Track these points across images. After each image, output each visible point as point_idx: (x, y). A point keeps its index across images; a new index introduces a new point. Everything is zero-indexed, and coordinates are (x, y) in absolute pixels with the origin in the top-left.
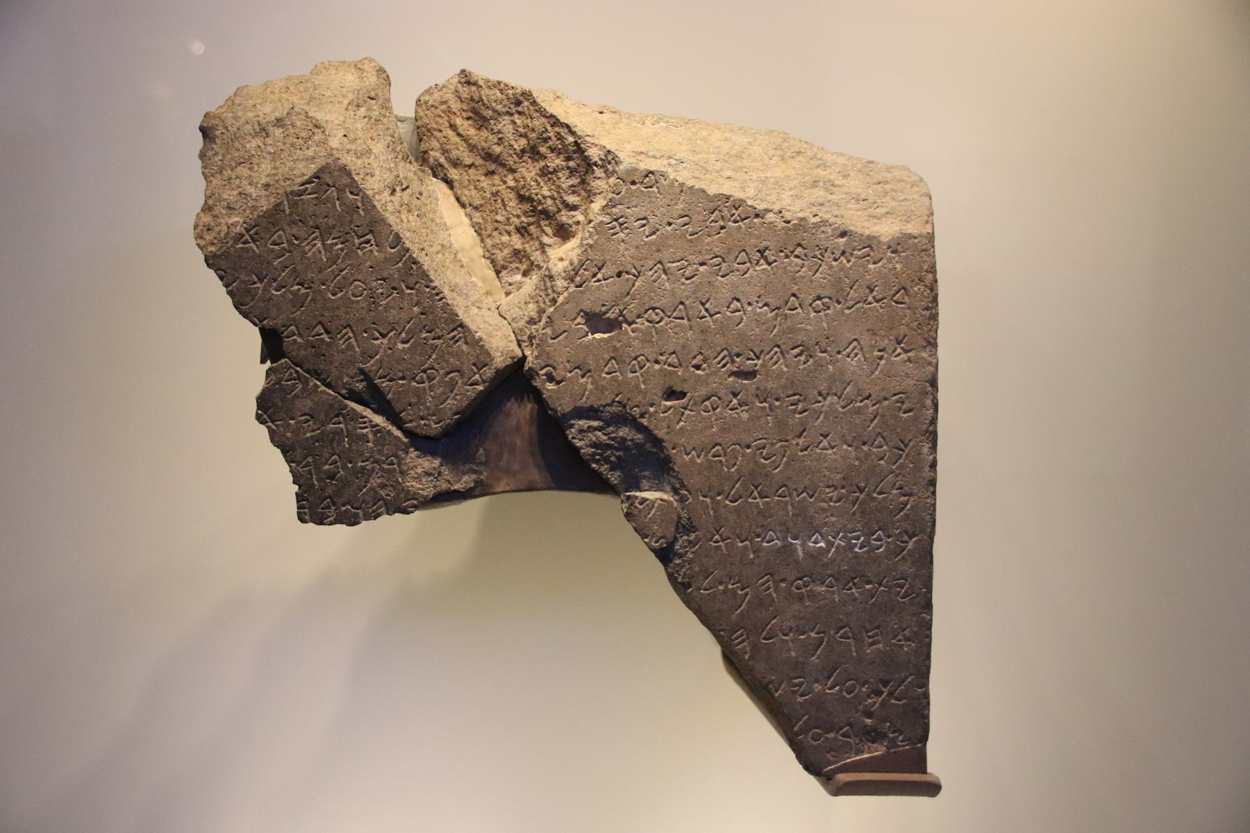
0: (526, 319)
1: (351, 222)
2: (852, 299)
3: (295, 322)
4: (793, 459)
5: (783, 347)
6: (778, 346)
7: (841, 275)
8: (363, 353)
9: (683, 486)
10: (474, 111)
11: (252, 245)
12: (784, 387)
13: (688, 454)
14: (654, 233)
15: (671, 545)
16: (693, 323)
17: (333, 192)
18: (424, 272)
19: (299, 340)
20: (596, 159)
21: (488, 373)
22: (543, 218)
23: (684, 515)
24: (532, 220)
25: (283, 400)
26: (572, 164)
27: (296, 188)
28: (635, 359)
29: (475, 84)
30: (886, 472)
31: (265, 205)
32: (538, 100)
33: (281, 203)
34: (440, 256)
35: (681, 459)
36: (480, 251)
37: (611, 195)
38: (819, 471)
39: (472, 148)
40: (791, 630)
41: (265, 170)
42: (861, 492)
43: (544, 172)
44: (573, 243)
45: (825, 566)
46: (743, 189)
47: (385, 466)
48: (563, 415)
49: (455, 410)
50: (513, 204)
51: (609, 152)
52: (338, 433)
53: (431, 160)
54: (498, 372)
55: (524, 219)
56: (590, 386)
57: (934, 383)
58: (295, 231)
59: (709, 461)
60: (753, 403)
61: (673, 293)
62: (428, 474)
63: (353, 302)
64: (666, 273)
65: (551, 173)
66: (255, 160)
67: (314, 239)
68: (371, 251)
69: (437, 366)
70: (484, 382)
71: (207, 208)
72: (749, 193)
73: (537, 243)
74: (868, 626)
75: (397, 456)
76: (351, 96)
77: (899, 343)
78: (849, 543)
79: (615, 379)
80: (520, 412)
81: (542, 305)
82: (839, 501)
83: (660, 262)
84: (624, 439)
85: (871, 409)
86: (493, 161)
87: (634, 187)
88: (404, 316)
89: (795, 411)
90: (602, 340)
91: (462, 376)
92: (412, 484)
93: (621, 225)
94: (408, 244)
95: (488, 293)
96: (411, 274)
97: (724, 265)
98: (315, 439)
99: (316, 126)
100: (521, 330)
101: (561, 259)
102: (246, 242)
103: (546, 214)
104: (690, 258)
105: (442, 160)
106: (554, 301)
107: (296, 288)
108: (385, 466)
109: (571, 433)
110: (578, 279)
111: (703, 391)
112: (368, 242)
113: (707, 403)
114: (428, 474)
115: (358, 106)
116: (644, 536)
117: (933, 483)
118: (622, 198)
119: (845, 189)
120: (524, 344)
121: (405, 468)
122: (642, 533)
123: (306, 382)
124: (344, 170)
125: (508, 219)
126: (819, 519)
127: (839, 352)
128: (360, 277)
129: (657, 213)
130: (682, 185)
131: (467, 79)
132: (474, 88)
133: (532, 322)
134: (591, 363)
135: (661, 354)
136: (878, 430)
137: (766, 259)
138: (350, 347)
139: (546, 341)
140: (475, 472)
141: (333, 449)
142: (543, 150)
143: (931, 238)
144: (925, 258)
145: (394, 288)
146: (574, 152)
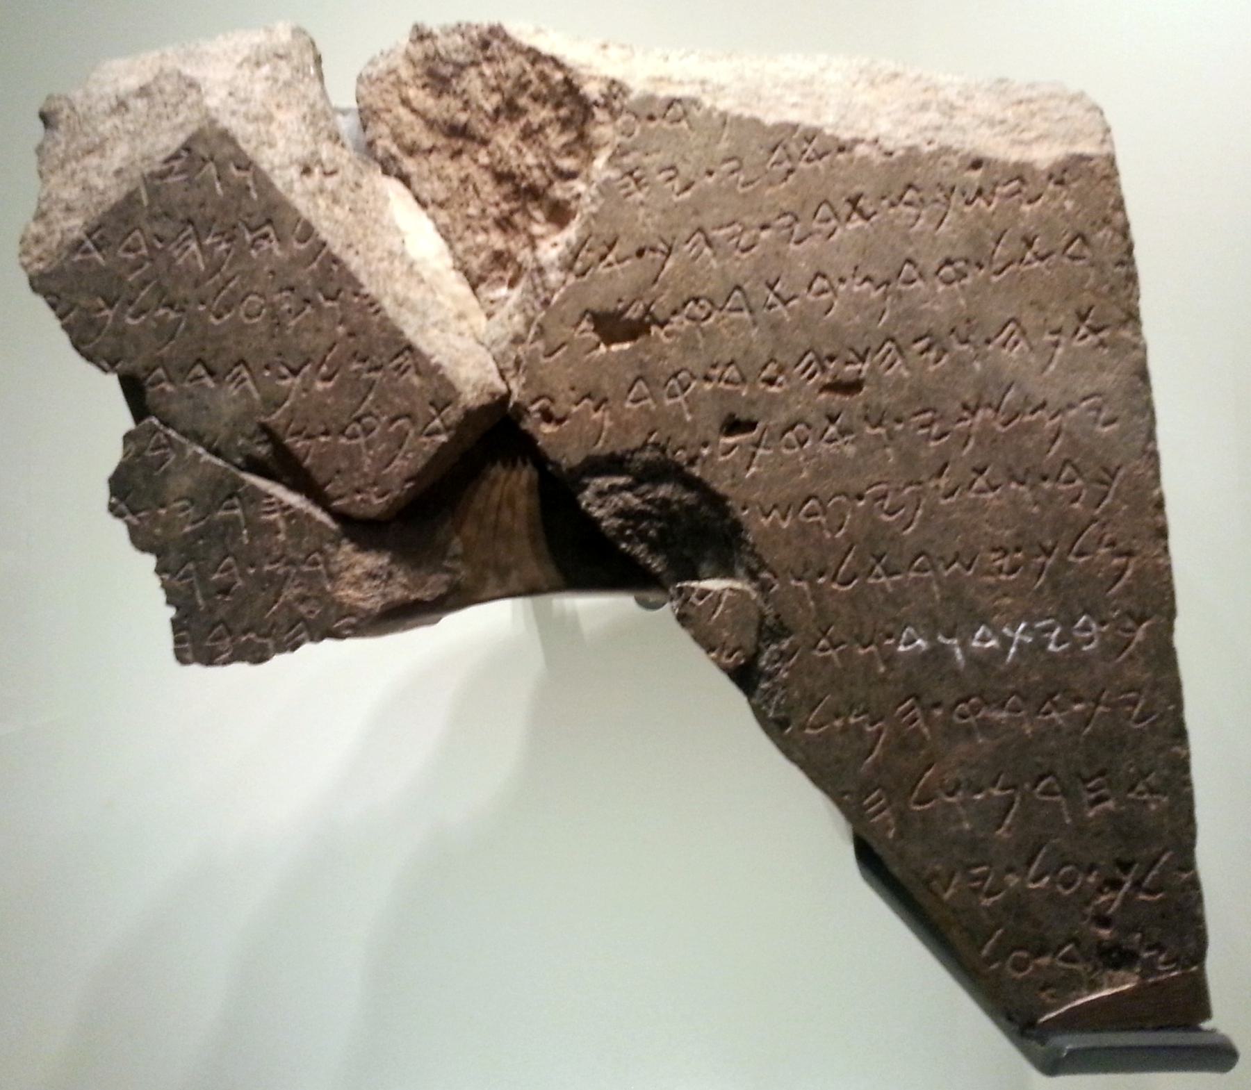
0: (510, 337)
1: (239, 209)
2: (1000, 259)
3: (161, 362)
4: (932, 511)
5: (900, 341)
6: (893, 340)
7: (980, 224)
8: (265, 400)
9: (763, 566)
10: (431, 73)
11: (97, 256)
12: (908, 401)
14: (687, 188)
15: (753, 659)
17: (211, 169)
21: (453, 415)
22: (528, 196)
23: (769, 611)
24: (514, 205)
25: (148, 478)
26: (563, 112)
27: (157, 168)
29: (430, 36)
30: (1086, 520)
31: (114, 196)
33: (137, 190)
34: (385, 264)
35: (757, 525)
36: (449, 261)
38: (975, 526)
39: (431, 124)
41: (119, 154)
42: (1048, 553)
43: (529, 134)
46: (818, 116)
47: (306, 569)
48: (571, 470)
49: (406, 475)
51: (613, 82)
53: (380, 153)
54: (469, 414)
55: (505, 207)
56: (608, 424)
57: (1143, 374)
58: (157, 228)
59: (800, 524)
60: (861, 430)
61: (723, 273)
62: (371, 576)
63: (246, 326)
66: (108, 145)
67: (185, 239)
68: (270, 251)
69: (376, 411)
70: (447, 429)
71: (41, 216)
72: (829, 121)
73: (524, 237)
75: (322, 552)
76: (246, 52)
77: (1083, 318)
79: (645, 410)
80: (511, 485)
81: (531, 313)
82: (1013, 570)
84: (666, 502)
85: (1049, 424)
86: (459, 134)
87: (652, 125)
88: (323, 341)
89: (928, 437)
90: (621, 352)
91: (414, 423)
92: (348, 594)
93: (637, 181)
94: (324, 236)
96: (331, 278)
98: (198, 535)
100: (504, 354)
101: (555, 245)
102: (87, 251)
103: (535, 193)
104: (747, 220)
105: (394, 150)
106: (546, 303)
107: (161, 312)
108: (306, 569)
110: (579, 266)
111: (782, 417)
112: (266, 236)
113: (789, 435)
115: (258, 64)
116: (710, 649)
117: (1162, 533)
120: (508, 375)
121: (335, 568)
122: (707, 642)
123: (181, 449)
124: (226, 137)
125: (484, 211)
126: (985, 602)
127: (988, 342)
128: (256, 288)
129: (690, 158)
130: (724, 115)
131: (421, 36)
132: (428, 43)
133: (517, 340)
134: (607, 386)
136: (1065, 456)
138: (246, 392)
139: (537, 360)
140: (447, 570)
141: (225, 548)
142: (523, 101)
144: (1109, 189)
145: (307, 301)
146: (565, 94)
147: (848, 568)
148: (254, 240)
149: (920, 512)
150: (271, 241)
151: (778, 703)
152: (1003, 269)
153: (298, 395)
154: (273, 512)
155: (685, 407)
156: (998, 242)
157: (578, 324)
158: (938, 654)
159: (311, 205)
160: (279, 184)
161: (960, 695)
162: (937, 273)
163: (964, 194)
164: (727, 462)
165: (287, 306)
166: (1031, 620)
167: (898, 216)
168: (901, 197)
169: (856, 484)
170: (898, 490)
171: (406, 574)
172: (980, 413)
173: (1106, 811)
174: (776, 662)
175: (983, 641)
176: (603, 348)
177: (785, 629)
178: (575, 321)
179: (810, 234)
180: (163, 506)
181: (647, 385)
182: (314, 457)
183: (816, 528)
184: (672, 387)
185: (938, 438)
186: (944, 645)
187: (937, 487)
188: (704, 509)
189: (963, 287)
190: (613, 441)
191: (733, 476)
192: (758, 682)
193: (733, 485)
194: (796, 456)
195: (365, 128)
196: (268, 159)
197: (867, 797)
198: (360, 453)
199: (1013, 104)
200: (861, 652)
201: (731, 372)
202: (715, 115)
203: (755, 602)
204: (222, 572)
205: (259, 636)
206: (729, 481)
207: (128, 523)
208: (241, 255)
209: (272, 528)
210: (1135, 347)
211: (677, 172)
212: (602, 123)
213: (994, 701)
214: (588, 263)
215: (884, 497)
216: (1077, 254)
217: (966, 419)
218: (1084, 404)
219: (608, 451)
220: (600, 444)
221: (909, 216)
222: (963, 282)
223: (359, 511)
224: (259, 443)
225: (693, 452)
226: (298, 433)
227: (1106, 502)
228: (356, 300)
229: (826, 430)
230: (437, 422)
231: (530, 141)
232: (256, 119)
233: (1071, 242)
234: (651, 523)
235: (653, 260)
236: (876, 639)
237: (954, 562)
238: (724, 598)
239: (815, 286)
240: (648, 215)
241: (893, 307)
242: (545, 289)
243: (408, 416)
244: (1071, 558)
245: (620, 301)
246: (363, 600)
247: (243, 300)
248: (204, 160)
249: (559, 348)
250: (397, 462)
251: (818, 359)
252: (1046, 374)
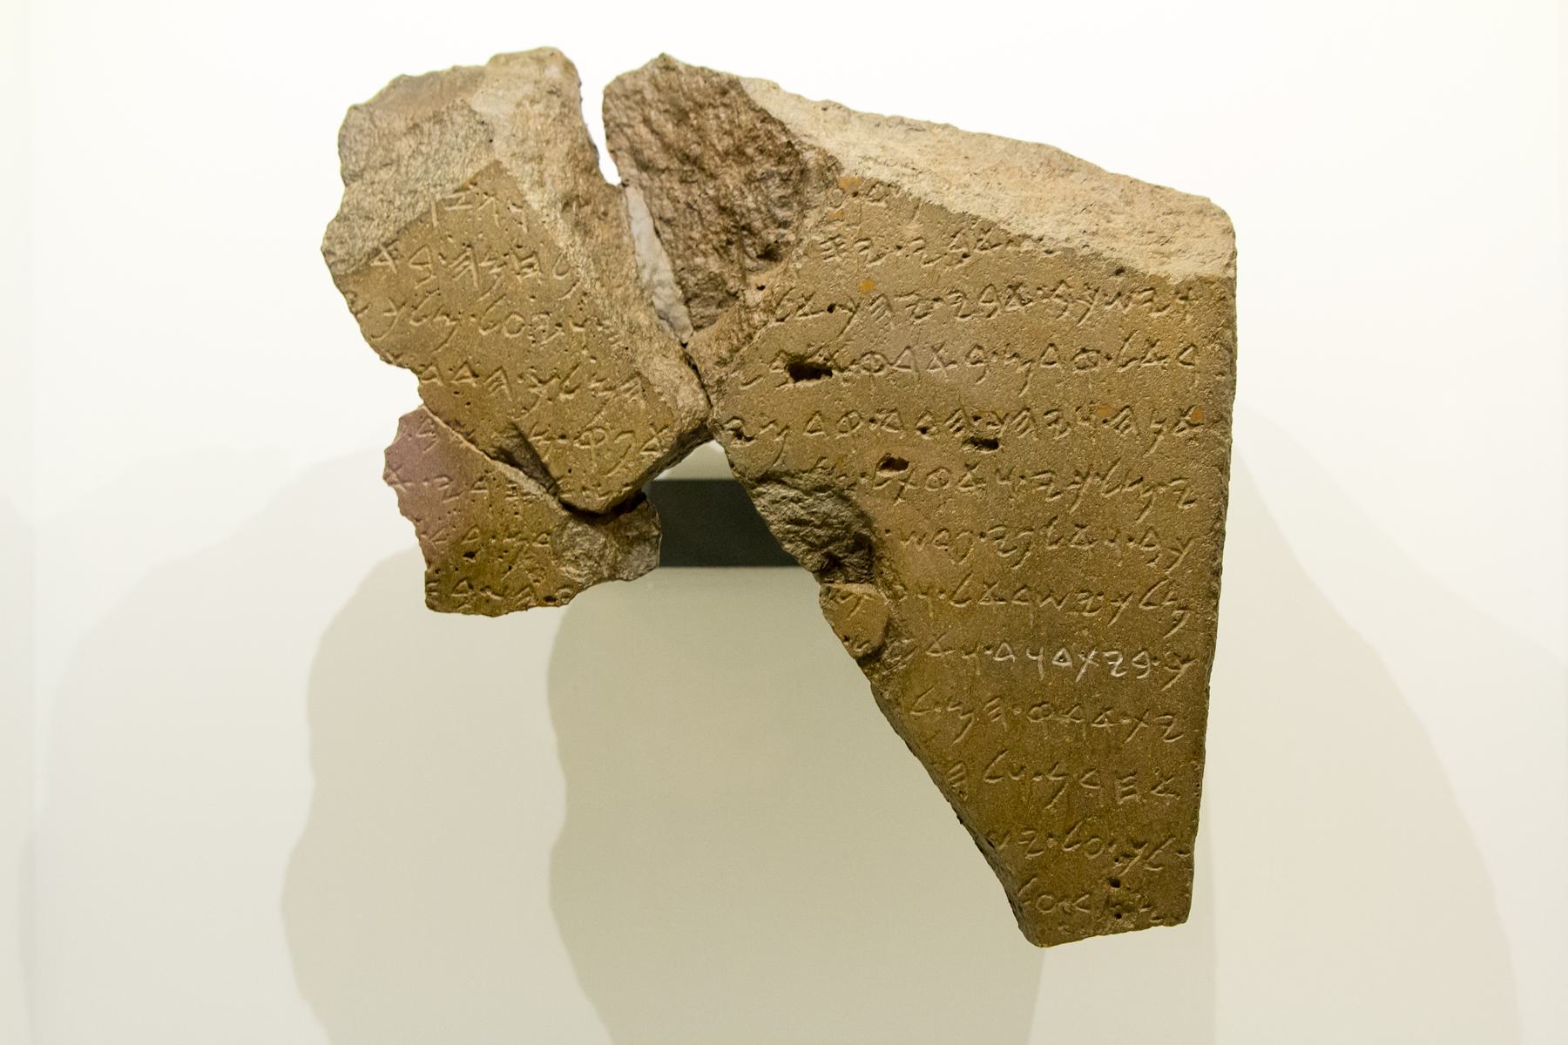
14: (879, 257)
26: (784, 169)
32: (749, 91)
39: (667, 147)
43: (749, 179)
50: (712, 216)
78: (1103, 664)
86: (692, 164)
90: (807, 389)
109: (760, 504)
117: (1215, 595)
118: (843, 212)
131: (666, 64)
132: (673, 74)
135: (879, 411)
142: (750, 151)
143: (1230, 283)
149: (1028, 554)
167: (1049, 305)
172: (1089, 480)
176: (790, 385)
210: (1221, 444)
221: (1057, 307)
223: (581, 505)
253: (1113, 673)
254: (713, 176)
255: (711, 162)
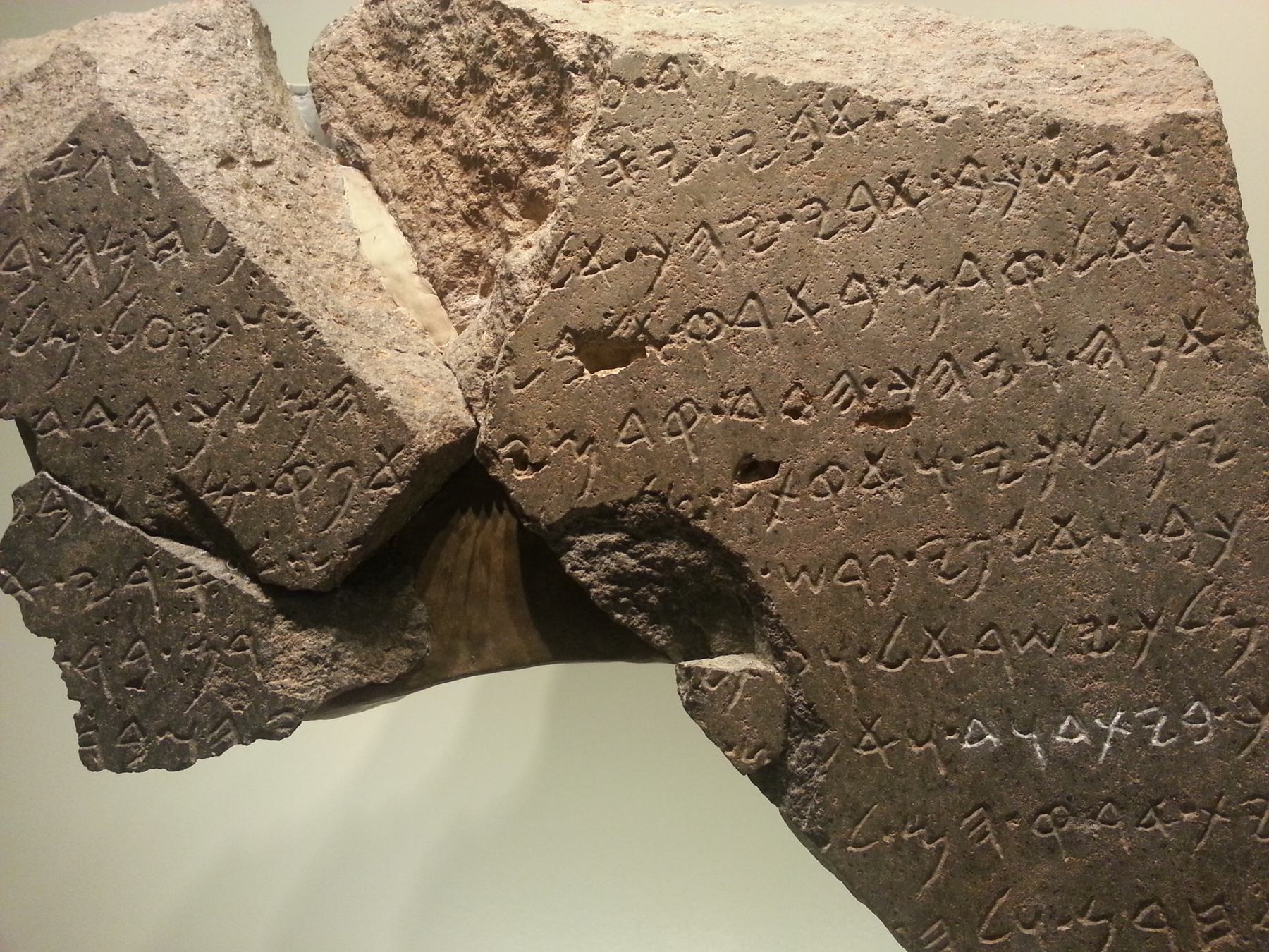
0: (478, 359)
3: (53, 404)
4: (1003, 571)
5: (958, 357)
6: (948, 357)
8: (176, 447)
9: (790, 642)
10: (388, 42)
12: (968, 434)
13: (794, 580)
14: (687, 172)
16: (778, 331)
17: (105, 165)
18: (274, 288)
19: (63, 434)
20: (574, 58)
21: (407, 461)
22: (499, 185)
25: (40, 545)
26: (536, 80)
28: (676, 408)
30: (1196, 582)
34: (332, 271)
35: (782, 592)
36: (412, 265)
37: (601, 110)
38: (1059, 591)
39: (389, 101)
40: (1038, 915)
42: (1151, 626)
43: (497, 109)
44: (552, 220)
45: (1094, 780)
47: (230, 653)
48: (550, 527)
51: (594, 38)
52: (141, 599)
53: (335, 137)
54: (426, 460)
55: (473, 198)
56: (595, 468)
59: (835, 587)
61: (733, 274)
62: (312, 659)
63: (151, 356)
64: (716, 242)
65: (505, 106)
68: (177, 260)
69: (311, 459)
70: (400, 479)
72: (862, 78)
74: (1199, 899)
77: (1190, 324)
79: (641, 451)
81: (501, 331)
83: (704, 224)
84: (669, 562)
89: (996, 478)
91: (359, 472)
93: (625, 163)
94: (241, 241)
95: (426, 331)
97: (826, 216)
98: (102, 613)
99: (87, 64)
100: (470, 380)
101: (528, 246)
103: (506, 182)
104: (761, 209)
105: (351, 133)
106: (518, 318)
107: (51, 341)
108: (230, 653)
110: (555, 271)
111: (812, 457)
112: (170, 245)
114: (312, 659)
115: (176, 37)
116: (726, 747)
119: (1035, 64)
121: (266, 653)
122: (722, 737)
125: (450, 203)
126: (1072, 686)
127: (1071, 356)
128: (160, 309)
129: (690, 133)
133: (486, 363)
134: (593, 423)
135: (724, 396)
137: (906, 194)
138: (153, 437)
140: (409, 644)
141: (134, 629)
142: (488, 69)
144: (1219, 158)
146: (537, 57)
147: (895, 647)
148: (158, 249)
150: (178, 250)
151: (812, 814)
152: (1088, 265)
153: (215, 440)
154: (191, 584)
155: (690, 446)
156: (1081, 230)
157: (557, 345)
158: (1013, 753)
159: (226, 204)
160: (185, 179)
161: (1040, 804)
162: (1004, 271)
163: (1037, 168)
164: (743, 513)
165: (199, 330)
166: (1128, 706)
168: (957, 175)
169: (904, 539)
170: (958, 546)
171: (357, 652)
172: (1062, 447)
173: (1225, 944)
174: (809, 761)
175: (1070, 735)
176: (587, 375)
177: (821, 721)
178: (551, 344)
179: (844, 225)
180: (61, 580)
181: (643, 422)
182: (237, 516)
183: (855, 595)
184: (674, 420)
185: (1007, 481)
186: (1020, 740)
187: (1009, 542)
188: (715, 570)
189: (1036, 287)
190: (602, 490)
191: (751, 531)
192: (788, 786)
193: (752, 542)
194: (829, 505)
195: (319, 109)
196: (171, 149)
197: (925, 931)
198: (294, 511)
199: (1085, 56)
200: (916, 750)
201: (747, 402)
202: (721, 75)
203: (781, 687)
204: (132, 659)
205: (177, 736)
206: (746, 538)
207: (19, 598)
208: (142, 268)
209: (189, 605)
211: (675, 152)
212: (582, 92)
213: (1085, 811)
214: (566, 268)
215: (941, 555)
216: (1183, 242)
217: (1044, 455)
218: (1193, 434)
219: (596, 503)
220: (587, 493)
222: (1038, 280)
224: (171, 500)
225: (700, 502)
226: (217, 487)
227: (1223, 557)
228: (283, 320)
229: (866, 471)
230: (387, 470)
231: (499, 118)
232: (164, 101)
233: (1174, 228)
234: (650, 589)
235: (646, 263)
236: (934, 735)
237: (1029, 638)
238: (743, 683)
239: (849, 290)
240: (640, 207)
241: (948, 315)
242: (517, 302)
243: (351, 463)
244: (1179, 630)
245: (607, 315)
246: (302, 691)
247: (145, 325)
248: (95, 152)
249: (533, 377)
250: (338, 521)
251: (855, 382)
252: (1146, 395)
253: (1154, 742)
254: (448, 121)
255: (442, 105)
